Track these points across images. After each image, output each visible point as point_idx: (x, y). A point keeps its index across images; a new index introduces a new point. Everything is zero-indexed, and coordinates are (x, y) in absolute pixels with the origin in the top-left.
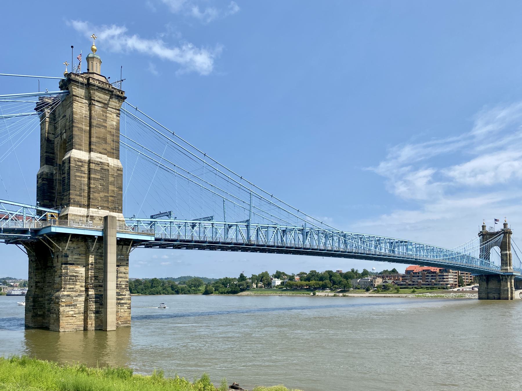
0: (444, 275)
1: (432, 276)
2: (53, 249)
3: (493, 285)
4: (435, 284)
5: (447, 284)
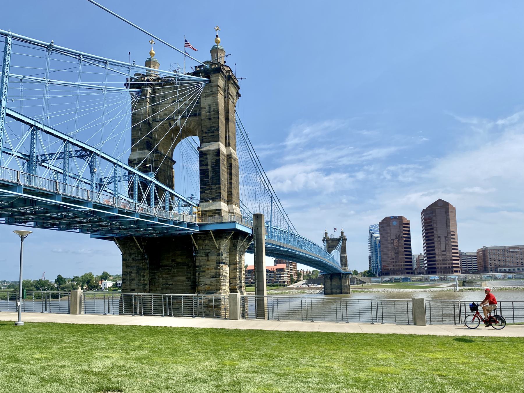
0: (280, 274)
1: (270, 275)
2: (197, 247)
3: (335, 282)
4: (275, 282)
5: (284, 282)
